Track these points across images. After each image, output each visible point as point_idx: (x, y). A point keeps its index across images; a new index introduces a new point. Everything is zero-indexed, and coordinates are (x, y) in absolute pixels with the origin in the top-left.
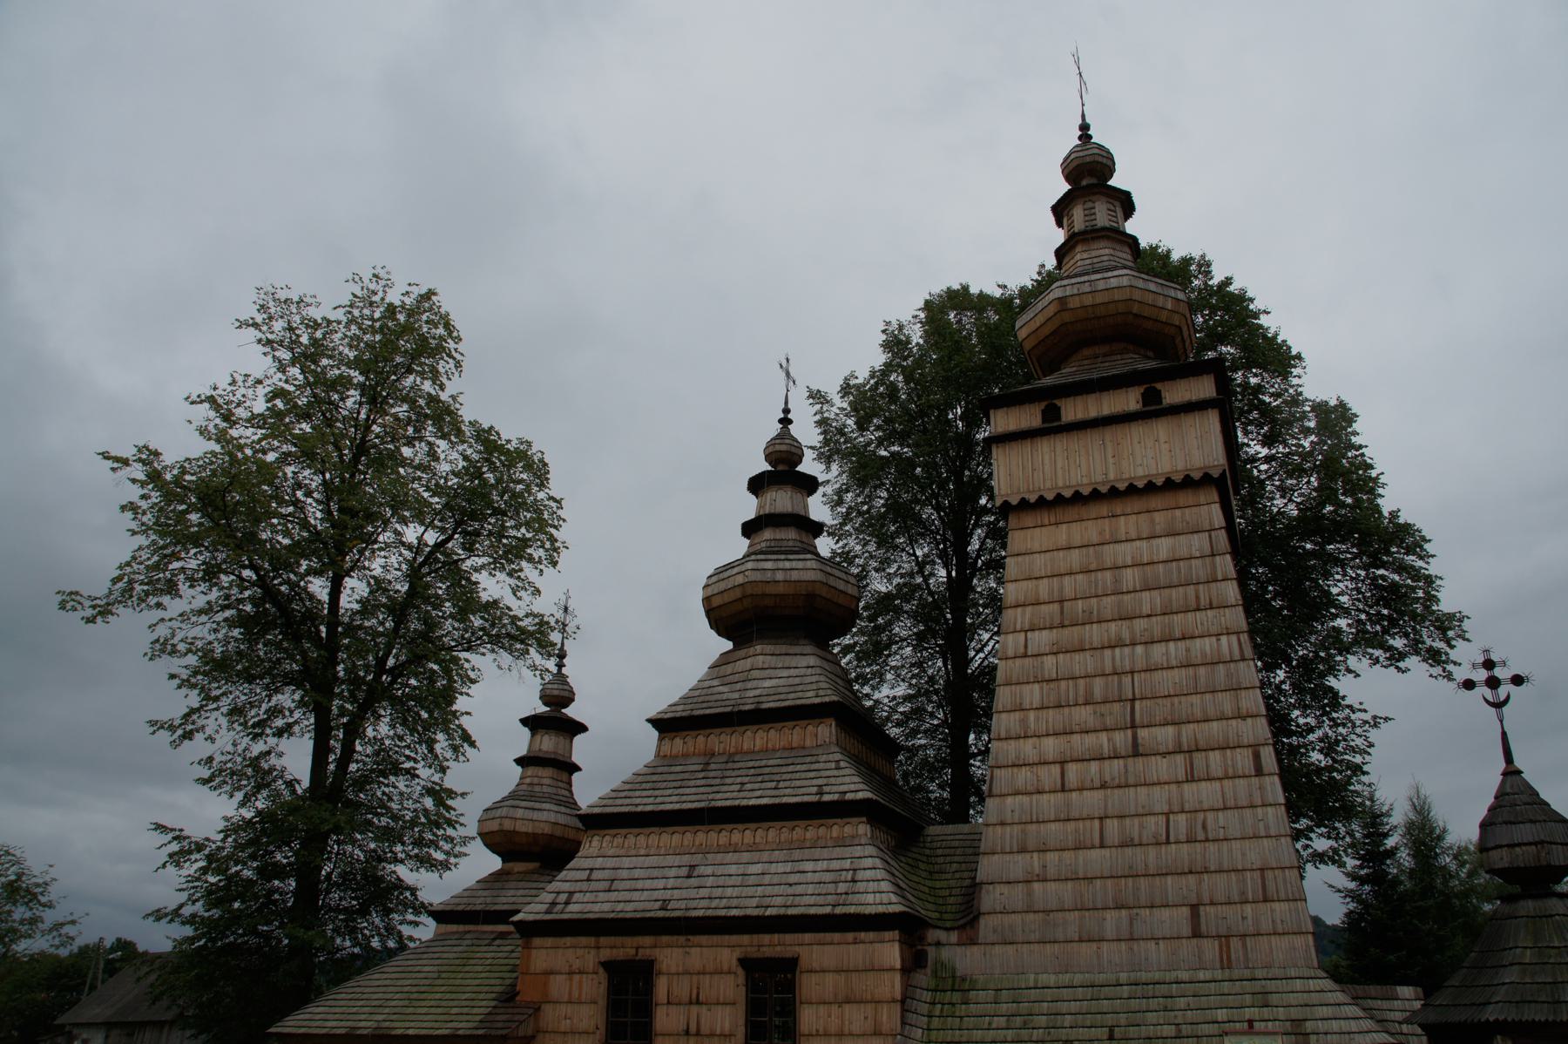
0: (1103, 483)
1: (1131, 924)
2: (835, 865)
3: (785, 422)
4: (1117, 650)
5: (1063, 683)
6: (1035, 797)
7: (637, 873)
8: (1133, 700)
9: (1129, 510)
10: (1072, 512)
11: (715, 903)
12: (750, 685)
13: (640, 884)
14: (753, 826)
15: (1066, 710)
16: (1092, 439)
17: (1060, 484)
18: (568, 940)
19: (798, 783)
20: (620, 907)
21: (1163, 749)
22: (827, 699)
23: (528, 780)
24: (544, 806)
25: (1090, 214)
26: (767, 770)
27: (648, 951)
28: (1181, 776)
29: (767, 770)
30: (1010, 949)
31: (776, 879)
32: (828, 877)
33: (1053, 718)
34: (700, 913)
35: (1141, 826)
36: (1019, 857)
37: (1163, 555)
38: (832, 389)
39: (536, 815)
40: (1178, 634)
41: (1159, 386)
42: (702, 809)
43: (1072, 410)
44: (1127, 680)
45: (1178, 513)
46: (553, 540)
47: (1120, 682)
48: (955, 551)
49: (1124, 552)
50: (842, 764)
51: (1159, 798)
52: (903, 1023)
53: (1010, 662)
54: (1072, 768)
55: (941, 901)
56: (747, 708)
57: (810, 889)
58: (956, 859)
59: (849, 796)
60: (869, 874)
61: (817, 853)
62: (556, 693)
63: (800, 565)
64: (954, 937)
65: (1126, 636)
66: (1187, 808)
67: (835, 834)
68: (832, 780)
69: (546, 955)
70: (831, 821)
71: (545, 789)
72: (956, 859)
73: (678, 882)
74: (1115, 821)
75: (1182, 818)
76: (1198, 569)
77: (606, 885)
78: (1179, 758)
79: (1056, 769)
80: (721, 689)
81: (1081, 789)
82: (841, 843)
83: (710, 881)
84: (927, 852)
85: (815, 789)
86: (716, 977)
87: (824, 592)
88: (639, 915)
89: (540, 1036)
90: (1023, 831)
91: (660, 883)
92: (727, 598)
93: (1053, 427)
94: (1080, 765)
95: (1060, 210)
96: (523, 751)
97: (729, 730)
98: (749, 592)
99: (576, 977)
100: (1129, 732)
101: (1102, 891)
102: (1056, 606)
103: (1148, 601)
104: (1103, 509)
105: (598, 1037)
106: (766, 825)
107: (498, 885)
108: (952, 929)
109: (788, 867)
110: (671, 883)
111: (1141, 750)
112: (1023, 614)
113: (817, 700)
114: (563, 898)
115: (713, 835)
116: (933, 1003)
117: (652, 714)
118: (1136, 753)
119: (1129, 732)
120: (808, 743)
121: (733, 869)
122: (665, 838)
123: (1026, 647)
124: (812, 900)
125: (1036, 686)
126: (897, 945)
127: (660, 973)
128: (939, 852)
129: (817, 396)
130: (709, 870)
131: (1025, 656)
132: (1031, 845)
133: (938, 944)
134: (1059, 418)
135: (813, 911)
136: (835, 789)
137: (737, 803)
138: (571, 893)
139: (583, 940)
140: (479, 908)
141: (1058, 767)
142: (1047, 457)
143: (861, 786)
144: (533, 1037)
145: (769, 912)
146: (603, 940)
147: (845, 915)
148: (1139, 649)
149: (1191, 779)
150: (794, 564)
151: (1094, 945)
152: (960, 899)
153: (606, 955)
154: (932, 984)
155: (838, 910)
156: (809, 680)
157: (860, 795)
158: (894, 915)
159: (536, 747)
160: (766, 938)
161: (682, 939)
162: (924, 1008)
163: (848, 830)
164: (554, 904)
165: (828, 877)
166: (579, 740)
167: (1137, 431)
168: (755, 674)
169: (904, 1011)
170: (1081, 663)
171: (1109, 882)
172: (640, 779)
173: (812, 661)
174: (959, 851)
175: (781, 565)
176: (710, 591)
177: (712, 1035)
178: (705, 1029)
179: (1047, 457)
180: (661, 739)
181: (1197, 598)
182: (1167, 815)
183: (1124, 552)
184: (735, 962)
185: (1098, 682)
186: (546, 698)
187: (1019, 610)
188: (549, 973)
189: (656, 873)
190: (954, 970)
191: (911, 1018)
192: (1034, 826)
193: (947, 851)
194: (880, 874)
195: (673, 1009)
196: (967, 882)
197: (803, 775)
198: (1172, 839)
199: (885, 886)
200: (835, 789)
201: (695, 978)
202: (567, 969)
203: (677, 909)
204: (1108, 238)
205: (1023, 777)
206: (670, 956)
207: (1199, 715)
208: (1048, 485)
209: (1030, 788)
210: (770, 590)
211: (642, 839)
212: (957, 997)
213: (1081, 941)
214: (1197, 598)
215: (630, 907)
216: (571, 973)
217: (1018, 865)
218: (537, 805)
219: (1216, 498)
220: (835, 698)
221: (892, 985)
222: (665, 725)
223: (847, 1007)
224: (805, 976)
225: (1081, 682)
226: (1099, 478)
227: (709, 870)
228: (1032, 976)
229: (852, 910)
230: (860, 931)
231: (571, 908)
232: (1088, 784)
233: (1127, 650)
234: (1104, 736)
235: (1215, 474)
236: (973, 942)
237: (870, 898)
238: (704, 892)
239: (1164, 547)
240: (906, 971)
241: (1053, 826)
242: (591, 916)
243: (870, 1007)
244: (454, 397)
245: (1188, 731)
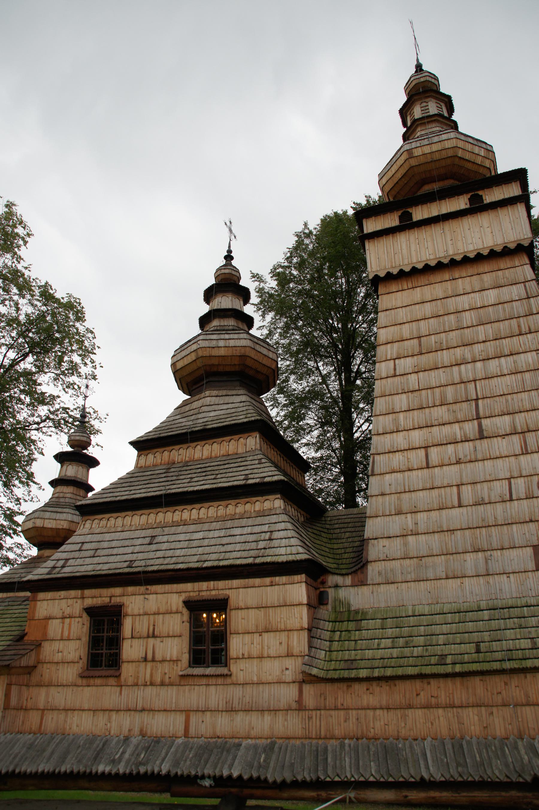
0: (445, 257)
1: (486, 562)
2: (257, 529)
3: (229, 257)
4: (463, 367)
5: (424, 392)
6: (406, 473)
7: (114, 544)
8: (477, 399)
9: (464, 274)
10: (423, 280)
11: (167, 561)
12: (200, 416)
13: (115, 551)
14: (198, 506)
15: (427, 410)
16: (436, 231)
17: (414, 261)
18: (63, 593)
19: (231, 474)
20: (99, 567)
21: (502, 432)
22: (253, 419)
23: (56, 495)
24: (65, 510)
25: (425, 109)
26: (210, 469)
27: (118, 600)
28: (518, 451)
29: (210, 469)
30: (392, 587)
31: (213, 542)
32: (251, 538)
33: (418, 417)
34: (155, 568)
35: (490, 489)
36: (397, 518)
37: (492, 301)
38: (265, 272)
39: (58, 516)
40: (507, 352)
41: (480, 193)
42: (161, 496)
43: (419, 213)
44: (471, 386)
45: (500, 273)
46: (93, 362)
47: (466, 389)
48: (344, 365)
49: (464, 302)
50: (263, 461)
51: (502, 468)
52: (310, 647)
53: (384, 381)
54: (434, 452)
55: (338, 557)
56: (197, 429)
57: (238, 547)
58: (349, 530)
59: (267, 479)
60: (282, 534)
61: (244, 522)
62: (78, 438)
63: (236, 336)
64: (348, 580)
65: (469, 358)
66: (524, 474)
67: (257, 509)
68: (256, 471)
69: (49, 605)
70: (254, 499)
71: (67, 500)
72: (349, 530)
73: (142, 548)
74: (469, 487)
75: (521, 481)
76: (519, 308)
77: (91, 553)
78: (516, 439)
79: (422, 452)
80: (181, 420)
81: (442, 466)
82: (262, 514)
83: (165, 546)
84: (328, 526)
85: (243, 477)
86: (167, 616)
87: (252, 354)
88: (111, 572)
89: (40, 666)
90: (399, 499)
91: (130, 550)
92: (186, 361)
93: (407, 225)
94: (439, 448)
95: (404, 112)
96: (55, 475)
97: (185, 446)
98: (200, 353)
99: (67, 621)
100: (476, 422)
101: (461, 540)
102: (416, 341)
103: (482, 332)
104: (446, 276)
105: (80, 665)
106: (207, 505)
107: (32, 565)
108: (347, 574)
109: (222, 533)
110: (137, 549)
111: (485, 434)
112: (392, 348)
113: (245, 420)
114: (61, 563)
115: (169, 514)
116: (334, 631)
117: (134, 438)
118: (482, 437)
119: (476, 422)
120: (240, 451)
121: (182, 537)
122: (136, 518)
123: (395, 369)
124: (238, 554)
125: (404, 396)
126: (304, 585)
127: (127, 615)
128: (337, 526)
129: (256, 277)
130: (165, 539)
131: (395, 376)
132: (405, 509)
133: (336, 586)
134: (412, 219)
135: (238, 562)
136: (257, 476)
137: (186, 489)
138: (67, 560)
139: (72, 593)
140: (16, 580)
141: (423, 451)
142: (404, 247)
143: (277, 473)
144: (35, 667)
145: (206, 565)
146: (87, 592)
147: (263, 564)
148: (479, 365)
149: (525, 452)
150: (232, 336)
151: (458, 581)
152: (352, 555)
153: (89, 602)
154: (332, 618)
155: (258, 561)
156: (241, 409)
157: (276, 478)
158: (301, 561)
159: (63, 474)
160: (204, 585)
161: (142, 589)
162: (327, 635)
163: (267, 505)
164: (54, 568)
165: (251, 538)
166: (92, 470)
167: (468, 222)
168: (204, 409)
169: (311, 637)
170: (435, 378)
171: (467, 532)
172: (122, 481)
173: (244, 398)
174: (350, 525)
175: (222, 336)
176: (175, 359)
177: (163, 661)
178: (158, 657)
179: (404, 247)
180: (139, 456)
181: (519, 326)
182: (509, 479)
183: (464, 302)
184: (181, 604)
185: (450, 390)
186: (71, 443)
187: (389, 345)
188: (50, 618)
189: (127, 543)
190: (349, 605)
191: (317, 643)
192: (407, 495)
193: (342, 525)
194: (290, 533)
195: (135, 642)
196: (357, 544)
197: (235, 469)
198: (514, 497)
199: (294, 541)
200: (257, 476)
201: (152, 617)
202: (60, 615)
203: (139, 566)
204: (438, 121)
205: (397, 460)
206: (136, 602)
207: (528, 406)
208: (406, 262)
209: (403, 468)
210: (215, 353)
211: (120, 520)
212: (352, 626)
213: (447, 578)
214: (519, 326)
215: (106, 567)
216: (63, 618)
217: (395, 524)
218: (60, 510)
219: (527, 261)
220: (259, 418)
221: (301, 617)
222: (142, 445)
223: (265, 635)
224: (233, 613)
225: (437, 390)
226: (442, 255)
227: (165, 539)
228: (410, 608)
229: (269, 559)
230: (275, 576)
231: (66, 570)
232: (446, 461)
233: (469, 366)
234: (456, 426)
235: (526, 243)
236: (363, 583)
237: (283, 551)
238: (159, 554)
239: (492, 296)
240: (309, 605)
241: (421, 494)
242: (78, 574)
243: (284, 635)
244: (26, 268)
245: (520, 419)
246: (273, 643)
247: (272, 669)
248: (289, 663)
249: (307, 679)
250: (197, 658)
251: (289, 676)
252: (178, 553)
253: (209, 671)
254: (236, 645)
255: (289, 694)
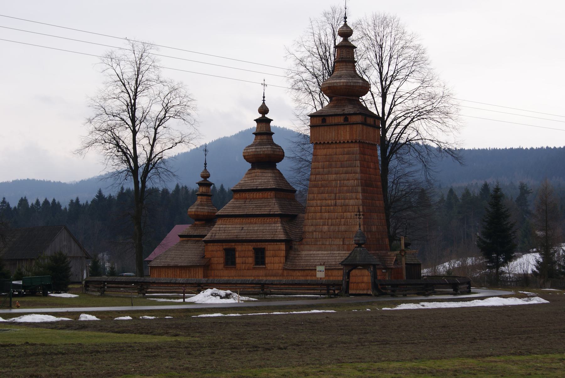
33: (320, 196)
59: (276, 213)
69: (211, 247)
104: (334, 146)
139: (220, 244)
146: (224, 244)
153: (225, 247)
157: (279, 213)
160: (259, 244)
163: (276, 220)
173: (270, 175)
221: (283, 253)
236: (301, 244)
240: (286, 250)
246: (276, 259)
247: (276, 266)
248: (281, 265)
249: (284, 269)
250: (257, 263)
251: (280, 268)
252: (251, 234)
253: (261, 266)
254: (267, 260)
255: (280, 272)
